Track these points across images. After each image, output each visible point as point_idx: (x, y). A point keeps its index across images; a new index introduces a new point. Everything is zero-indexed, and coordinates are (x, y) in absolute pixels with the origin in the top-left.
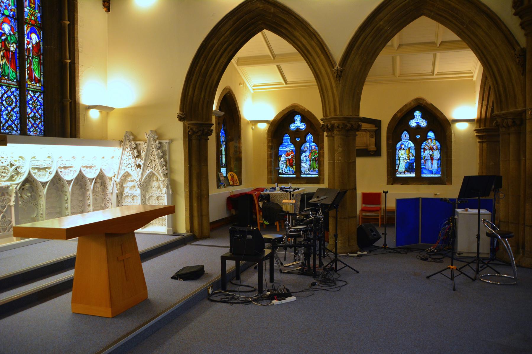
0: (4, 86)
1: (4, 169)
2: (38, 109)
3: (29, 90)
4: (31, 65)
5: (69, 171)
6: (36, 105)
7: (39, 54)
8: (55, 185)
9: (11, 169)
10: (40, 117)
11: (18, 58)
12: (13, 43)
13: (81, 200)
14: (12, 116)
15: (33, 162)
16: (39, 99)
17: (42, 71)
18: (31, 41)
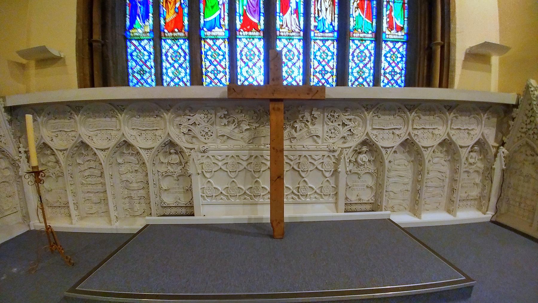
2: (398, 62)
4: (391, 11)
10: (400, 71)
11: (374, 6)
14: (364, 72)
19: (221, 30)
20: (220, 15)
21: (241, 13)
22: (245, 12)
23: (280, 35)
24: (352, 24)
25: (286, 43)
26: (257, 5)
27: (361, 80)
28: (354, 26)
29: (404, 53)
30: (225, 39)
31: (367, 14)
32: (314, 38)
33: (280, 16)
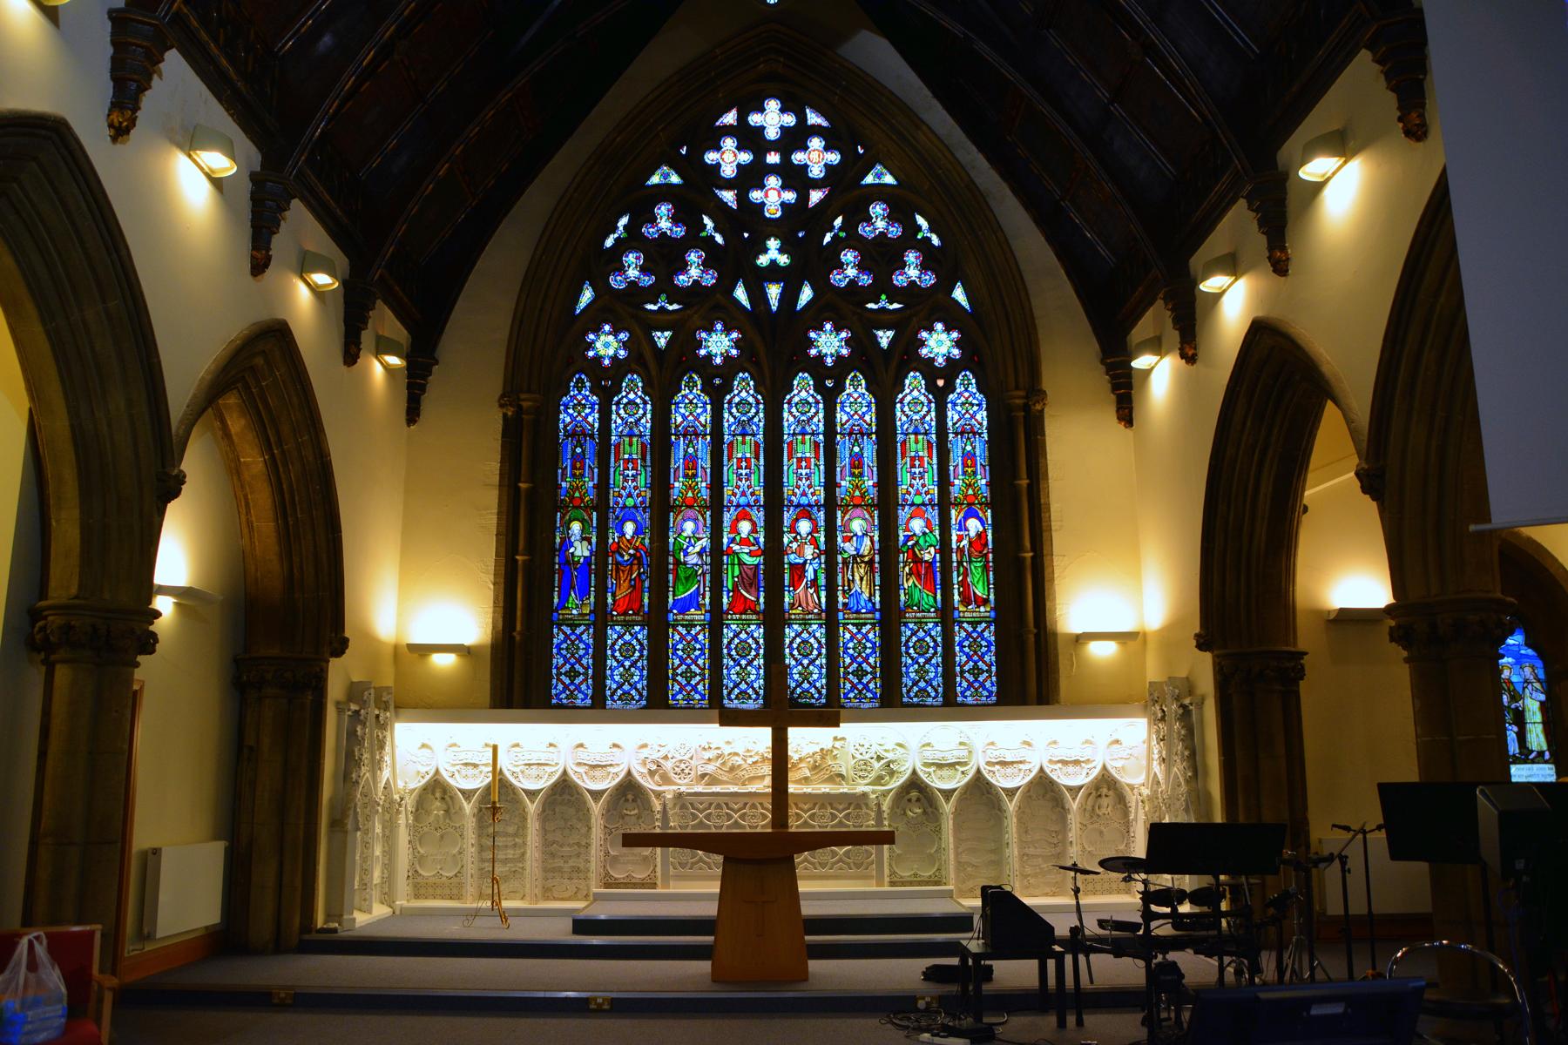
0: (911, 622)
1: (865, 764)
3: (963, 622)
4: (966, 574)
5: (1016, 770)
6: (978, 646)
7: (985, 552)
8: (984, 797)
9: (877, 765)
12: (928, 546)
13: (1056, 832)
14: (927, 672)
15: (927, 754)
16: (986, 634)
17: (991, 582)
18: (967, 533)
19: (700, 612)
20: (698, 588)
21: (730, 587)
22: (735, 585)
23: (790, 619)
24: (902, 597)
25: (800, 629)
26: (754, 575)
27: (922, 684)
28: (905, 603)
29: (993, 638)
30: (705, 625)
31: (925, 583)
32: (843, 621)
33: (789, 591)
